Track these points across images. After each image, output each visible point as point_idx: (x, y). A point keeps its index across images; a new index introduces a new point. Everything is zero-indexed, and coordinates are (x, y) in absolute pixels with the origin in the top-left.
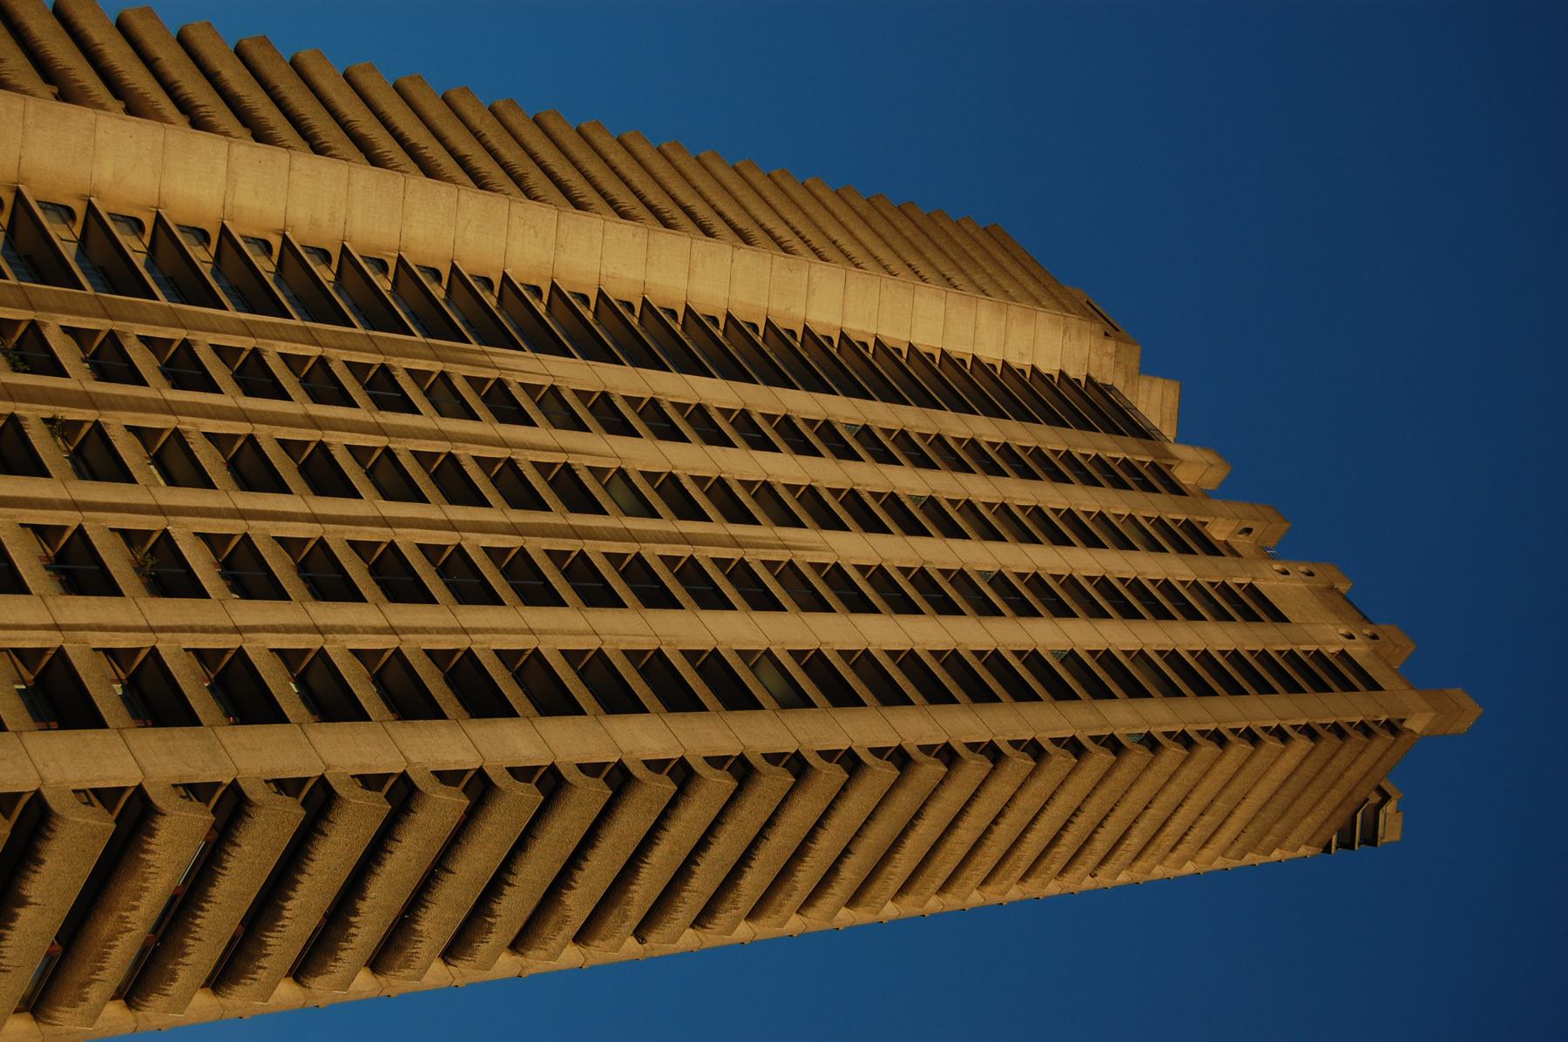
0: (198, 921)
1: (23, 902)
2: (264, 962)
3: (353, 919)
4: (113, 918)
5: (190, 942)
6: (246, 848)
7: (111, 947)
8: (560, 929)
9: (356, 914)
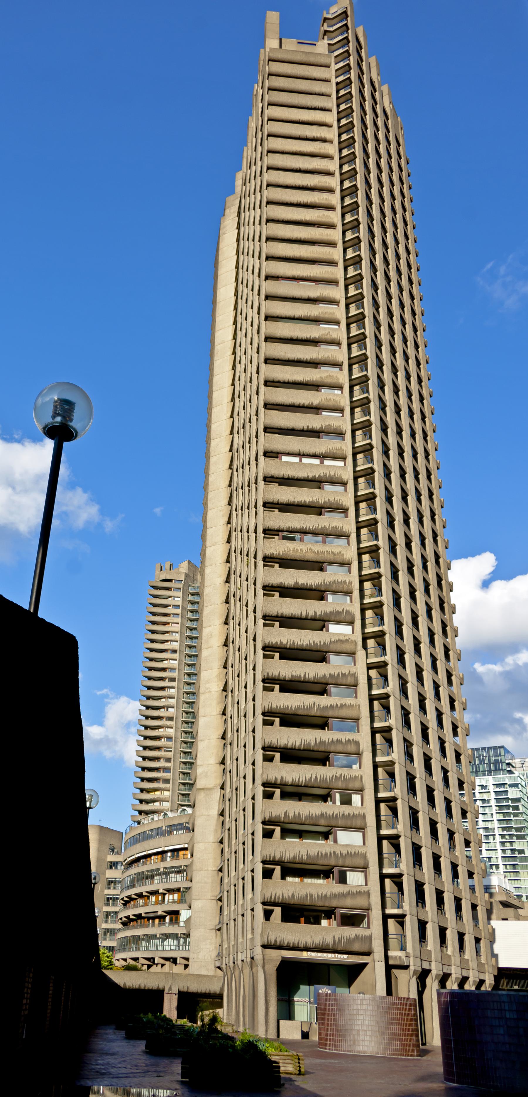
0: (311, 527)
1: (297, 583)
2: (332, 499)
3: (317, 476)
4: (306, 554)
5: (320, 527)
6: (280, 524)
7: (318, 551)
8: (330, 399)
9: (315, 476)
